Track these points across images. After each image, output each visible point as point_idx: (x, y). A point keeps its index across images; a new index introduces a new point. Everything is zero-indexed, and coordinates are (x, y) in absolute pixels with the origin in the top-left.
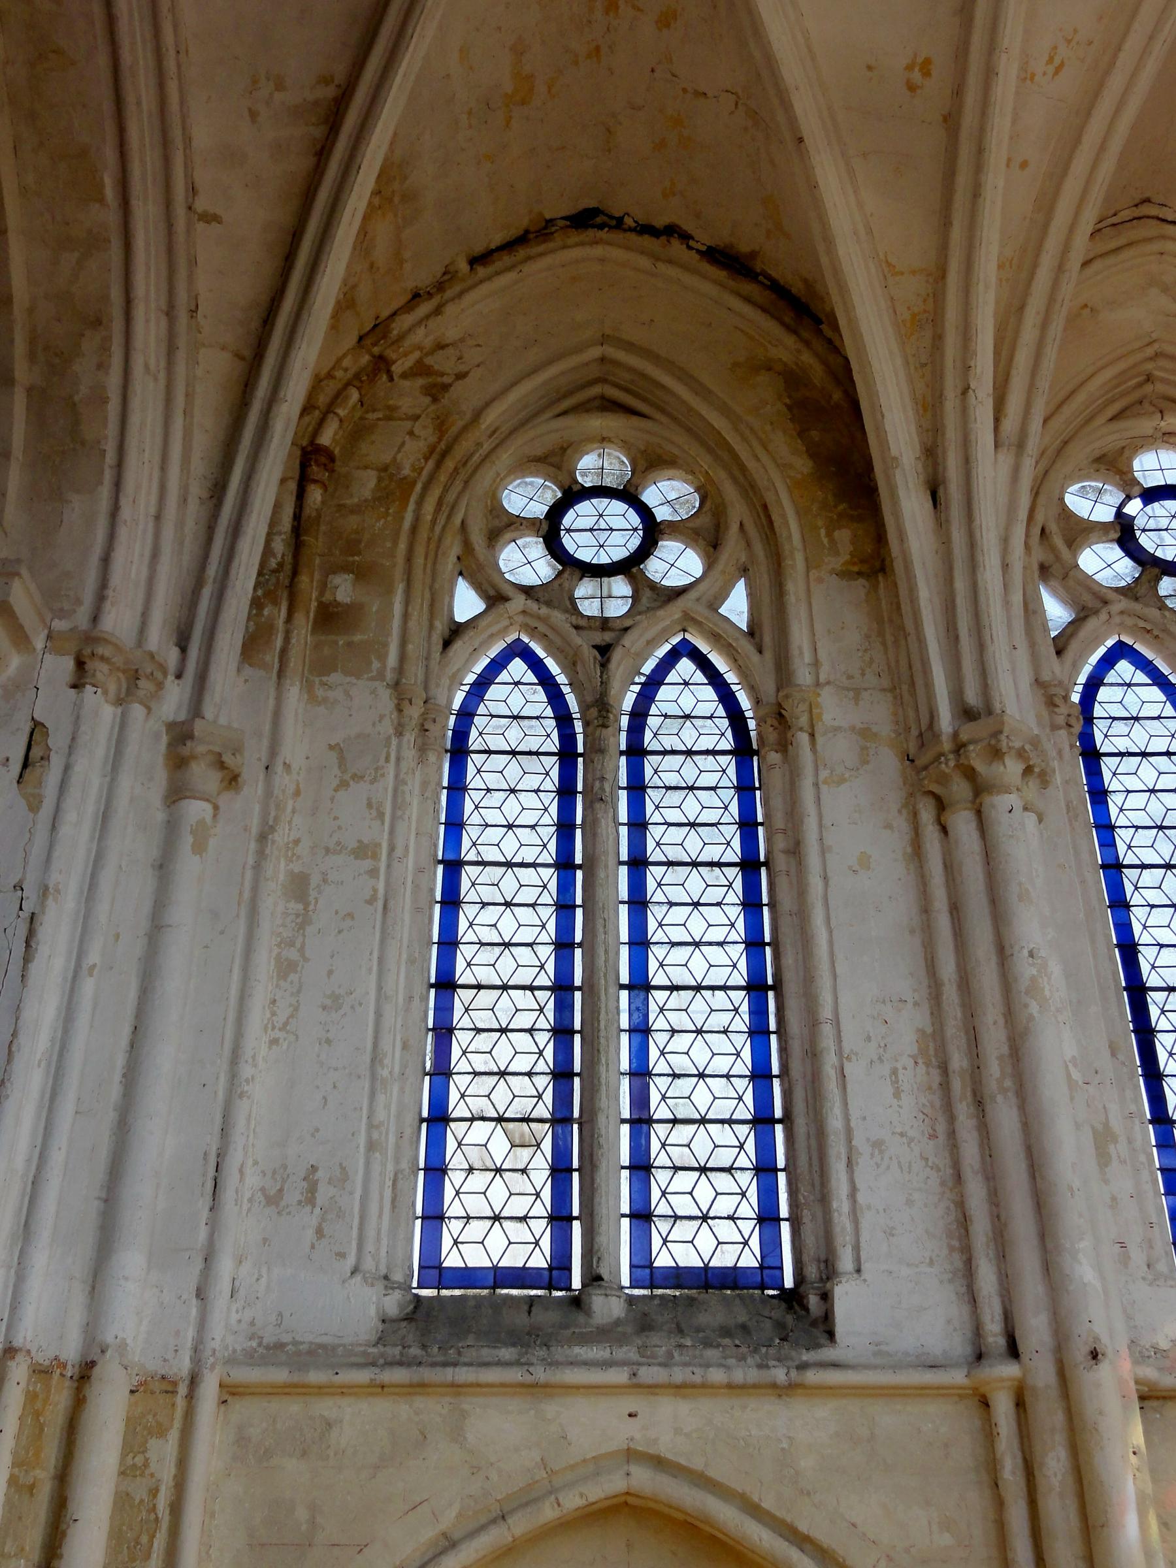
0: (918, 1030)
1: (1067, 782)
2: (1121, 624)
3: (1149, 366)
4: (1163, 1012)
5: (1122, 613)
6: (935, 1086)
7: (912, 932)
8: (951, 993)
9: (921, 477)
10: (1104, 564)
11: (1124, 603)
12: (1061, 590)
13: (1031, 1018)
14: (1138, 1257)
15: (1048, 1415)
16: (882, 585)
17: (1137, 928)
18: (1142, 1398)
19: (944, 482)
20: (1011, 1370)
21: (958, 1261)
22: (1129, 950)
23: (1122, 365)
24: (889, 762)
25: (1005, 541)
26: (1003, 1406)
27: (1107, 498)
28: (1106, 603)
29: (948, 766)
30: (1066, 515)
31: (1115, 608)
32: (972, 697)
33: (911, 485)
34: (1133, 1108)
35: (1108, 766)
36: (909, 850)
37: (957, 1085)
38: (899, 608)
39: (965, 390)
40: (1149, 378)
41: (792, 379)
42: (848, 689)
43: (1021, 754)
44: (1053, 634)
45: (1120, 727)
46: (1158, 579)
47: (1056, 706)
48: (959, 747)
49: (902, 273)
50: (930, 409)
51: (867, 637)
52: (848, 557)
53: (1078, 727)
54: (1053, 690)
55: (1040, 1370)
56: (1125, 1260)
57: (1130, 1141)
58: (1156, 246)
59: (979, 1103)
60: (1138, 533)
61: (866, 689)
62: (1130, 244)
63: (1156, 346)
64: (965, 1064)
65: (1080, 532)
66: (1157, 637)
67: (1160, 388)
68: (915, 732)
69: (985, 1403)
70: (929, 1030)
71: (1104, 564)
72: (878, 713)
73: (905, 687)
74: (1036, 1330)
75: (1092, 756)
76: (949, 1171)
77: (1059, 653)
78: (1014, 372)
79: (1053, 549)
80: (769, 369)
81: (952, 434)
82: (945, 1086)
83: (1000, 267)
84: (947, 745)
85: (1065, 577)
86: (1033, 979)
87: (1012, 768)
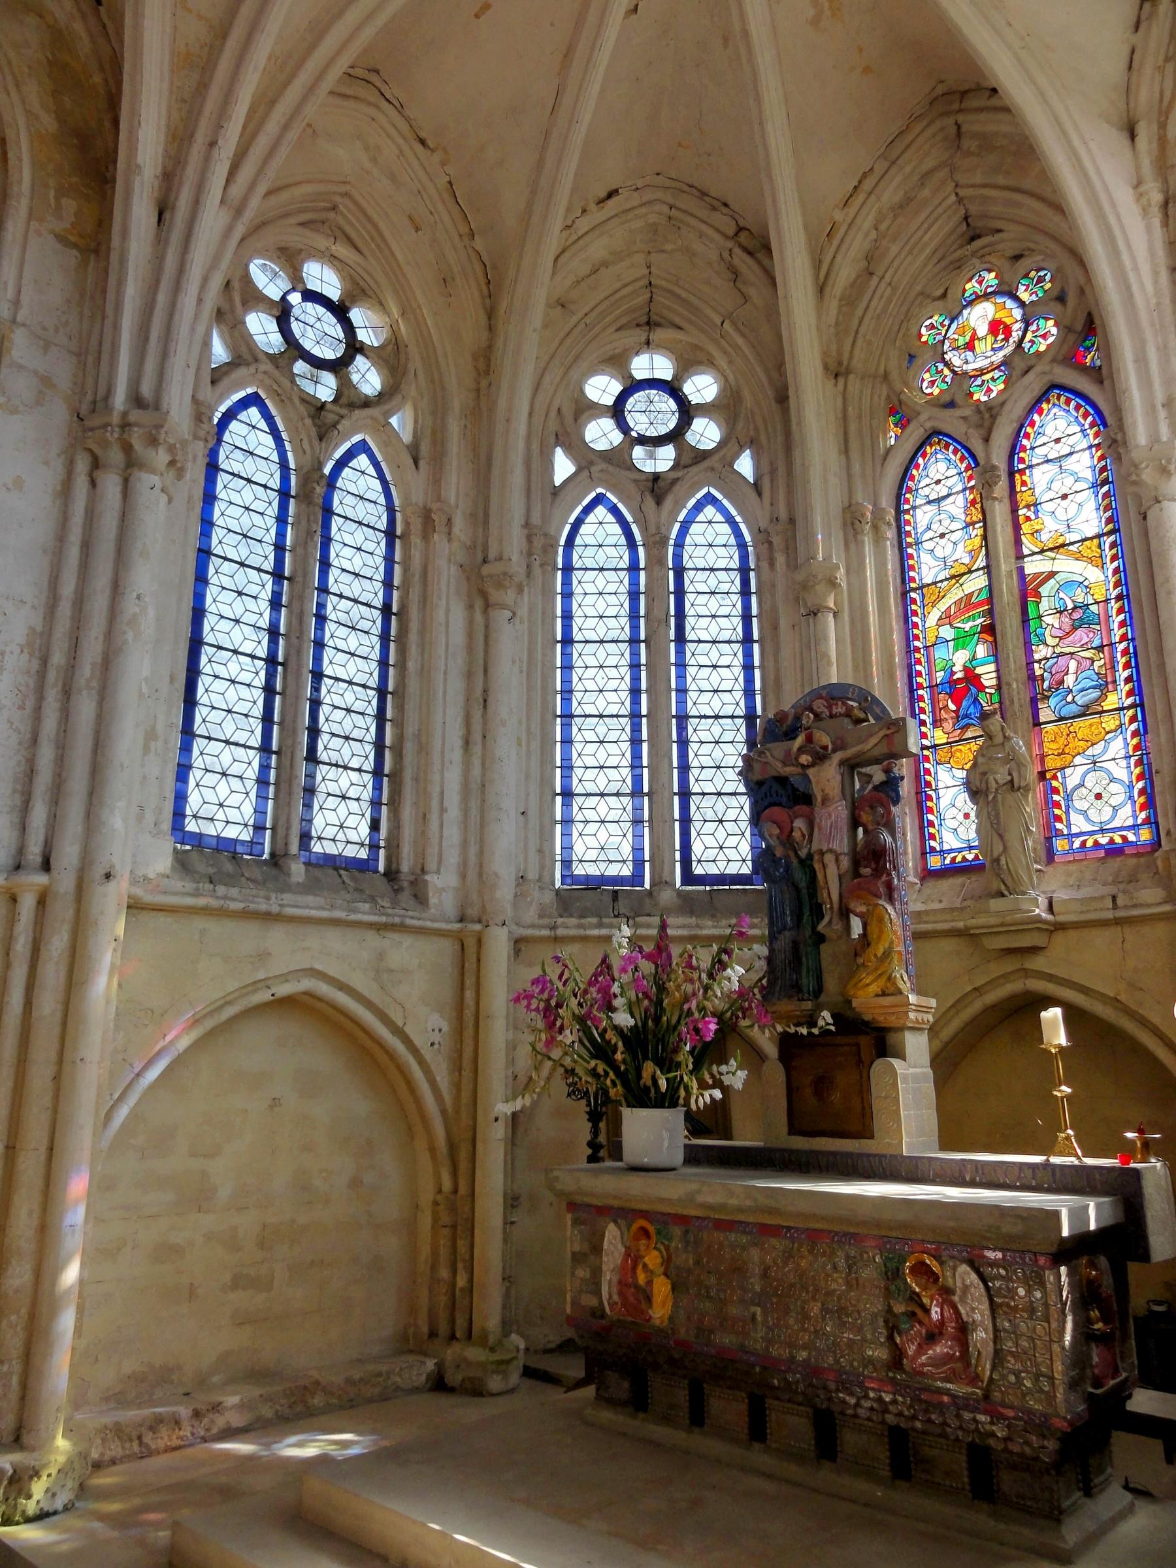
0: (30, 628)
1: (194, 481)
2: (262, 381)
3: (338, 199)
4: (210, 661)
5: (265, 373)
6: (33, 671)
7: (45, 551)
8: (65, 609)
9: (156, 194)
10: (262, 329)
11: (267, 366)
12: (227, 336)
13: (125, 642)
14: (150, 818)
15: (62, 911)
16: (92, 264)
17: (209, 600)
18: (128, 907)
19: (173, 208)
20: (42, 879)
21: (18, 800)
22: (198, 613)
23: (322, 188)
24: (59, 414)
25: (205, 280)
26: (28, 903)
27: (279, 281)
28: (256, 360)
29: (113, 435)
30: (247, 279)
31: (262, 367)
32: (146, 390)
33: (145, 194)
34: (174, 721)
35: (222, 479)
36: (59, 488)
37: (52, 675)
38: (104, 291)
39: (212, 144)
40: (334, 208)
41: (58, 38)
42: (40, 338)
43: (171, 449)
44: (213, 366)
45: (238, 454)
46: (295, 360)
47: (201, 422)
48: (125, 425)
49: (190, 11)
50: (179, 141)
51: (68, 301)
52: (68, 226)
53: (211, 445)
54: (203, 409)
55: (64, 879)
56: (140, 818)
57: (166, 742)
58: (372, 112)
59: (67, 693)
60: (292, 319)
61: (56, 345)
62: (356, 98)
63: (347, 188)
64: (63, 662)
65: (254, 298)
66: (283, 401)
67: (341, 222)
68: (89, 397)
69: (14, 899)
70: (39, 629)
71: (262, 329)
72: (63, 371)
73: (90, 359)
74: (68, 855)
75: (213, 469)
76: (28, 736)
77: (213, 382)
78: (252, 151)
79: (231, 300)
80: (41, 16)
81: (190, 173)
82: (42, 674)
83: (269, 59)
84: (116, 419)
85: (234, 327)
86: (135, 615)
87: (161, 457)
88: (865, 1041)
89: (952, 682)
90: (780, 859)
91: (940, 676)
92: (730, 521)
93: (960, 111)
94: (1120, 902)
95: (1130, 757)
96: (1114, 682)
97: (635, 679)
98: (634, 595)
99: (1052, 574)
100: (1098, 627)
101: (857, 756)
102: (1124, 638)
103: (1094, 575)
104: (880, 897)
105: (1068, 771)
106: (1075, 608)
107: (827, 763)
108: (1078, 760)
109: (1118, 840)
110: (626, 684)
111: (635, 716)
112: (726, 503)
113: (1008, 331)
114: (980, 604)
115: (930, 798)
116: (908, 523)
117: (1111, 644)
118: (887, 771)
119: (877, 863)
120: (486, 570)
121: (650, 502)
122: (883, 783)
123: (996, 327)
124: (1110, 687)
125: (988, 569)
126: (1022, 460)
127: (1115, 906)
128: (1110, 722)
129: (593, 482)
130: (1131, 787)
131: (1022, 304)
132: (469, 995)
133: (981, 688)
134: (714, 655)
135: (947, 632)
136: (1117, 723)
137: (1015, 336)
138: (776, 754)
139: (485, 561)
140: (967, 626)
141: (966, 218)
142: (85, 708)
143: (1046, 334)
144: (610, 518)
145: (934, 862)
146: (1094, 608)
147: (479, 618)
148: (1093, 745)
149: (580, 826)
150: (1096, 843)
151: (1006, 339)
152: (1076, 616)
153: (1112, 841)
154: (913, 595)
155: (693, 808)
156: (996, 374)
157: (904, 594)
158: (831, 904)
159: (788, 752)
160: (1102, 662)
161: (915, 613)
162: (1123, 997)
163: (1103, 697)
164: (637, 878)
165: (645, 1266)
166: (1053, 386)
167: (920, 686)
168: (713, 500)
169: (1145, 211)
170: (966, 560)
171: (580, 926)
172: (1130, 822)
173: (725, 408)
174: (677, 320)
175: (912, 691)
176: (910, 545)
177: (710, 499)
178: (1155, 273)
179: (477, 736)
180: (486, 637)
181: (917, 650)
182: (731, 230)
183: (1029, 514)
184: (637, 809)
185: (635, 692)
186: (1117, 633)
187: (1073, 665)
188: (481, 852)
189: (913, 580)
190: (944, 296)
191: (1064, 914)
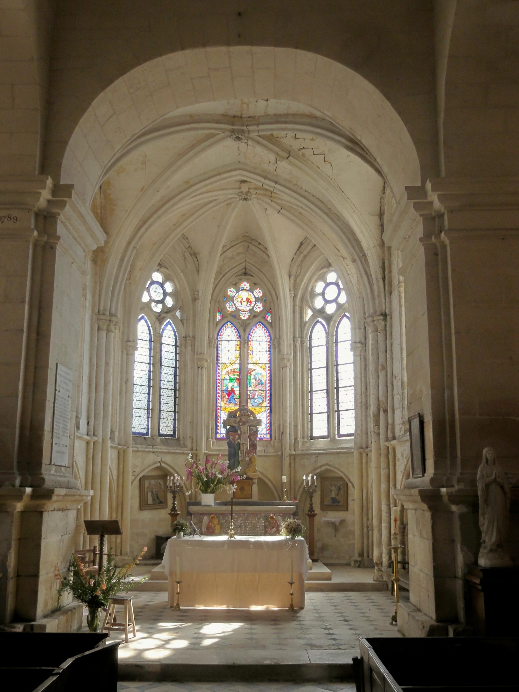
15: (99, 447)
88: (250, 481)
89: (227, 391)
91: (224, 388)
92: (174, 331)
93: (250, 243)
97: (150, 375)
98: (150, 349)
99: (254, 370)
103: (264, 373)
110: (147, 377)
111: (149, 386)
112: (173, 324)
113: (251, 303)
114: (237, 372)
115: (218, 419)
116: (220, 344)
120: (129, 344)
121: (157, 323)
123: (248, 300)
125: (241, 364)
126: (251, 338)
129: (143, 313)
130: (266, 425)
131: (255, 297)
132: (121, 466)
133: (235, 394)
134: (168, 371)
135: (227, 377)
137: (252, 305)
139: (128, 341)
140: (233, 377)
141: (245, 268)
142: (102, 395)
143: (259, 307)
144: (145, 324)
145: (218, 436)
147: (125, 356)
149: (134, 417)
151: (250, 304)
152: (259, 382)
154: (219, 364)
155: (161, 415)
156: (247, 313)
157: (217, 363)
161: (219, 369)
162: (264, 472)
164: (147, 434)
165: (214, 524)
166: (260, 322)
167: (219, 389)
168: (170, 324)
169: (290, 298)
170: (234, 359)
171: (142, 448)
173: (174, 295)
174: (168, 267)
175: (217, 390)
176: (219, 350)
177: (169, 323)
178: (291, 313)
179: (124, 393)
180: (127, 363)
181: (219, 380)
182: (187, 246)
183: (251, 353)
184: (148, 413)
185: (149, 379)
186: (268, 388)
187: (257, 393)
188: (125, 426)
189: (219, 360)
190: (236, 284)
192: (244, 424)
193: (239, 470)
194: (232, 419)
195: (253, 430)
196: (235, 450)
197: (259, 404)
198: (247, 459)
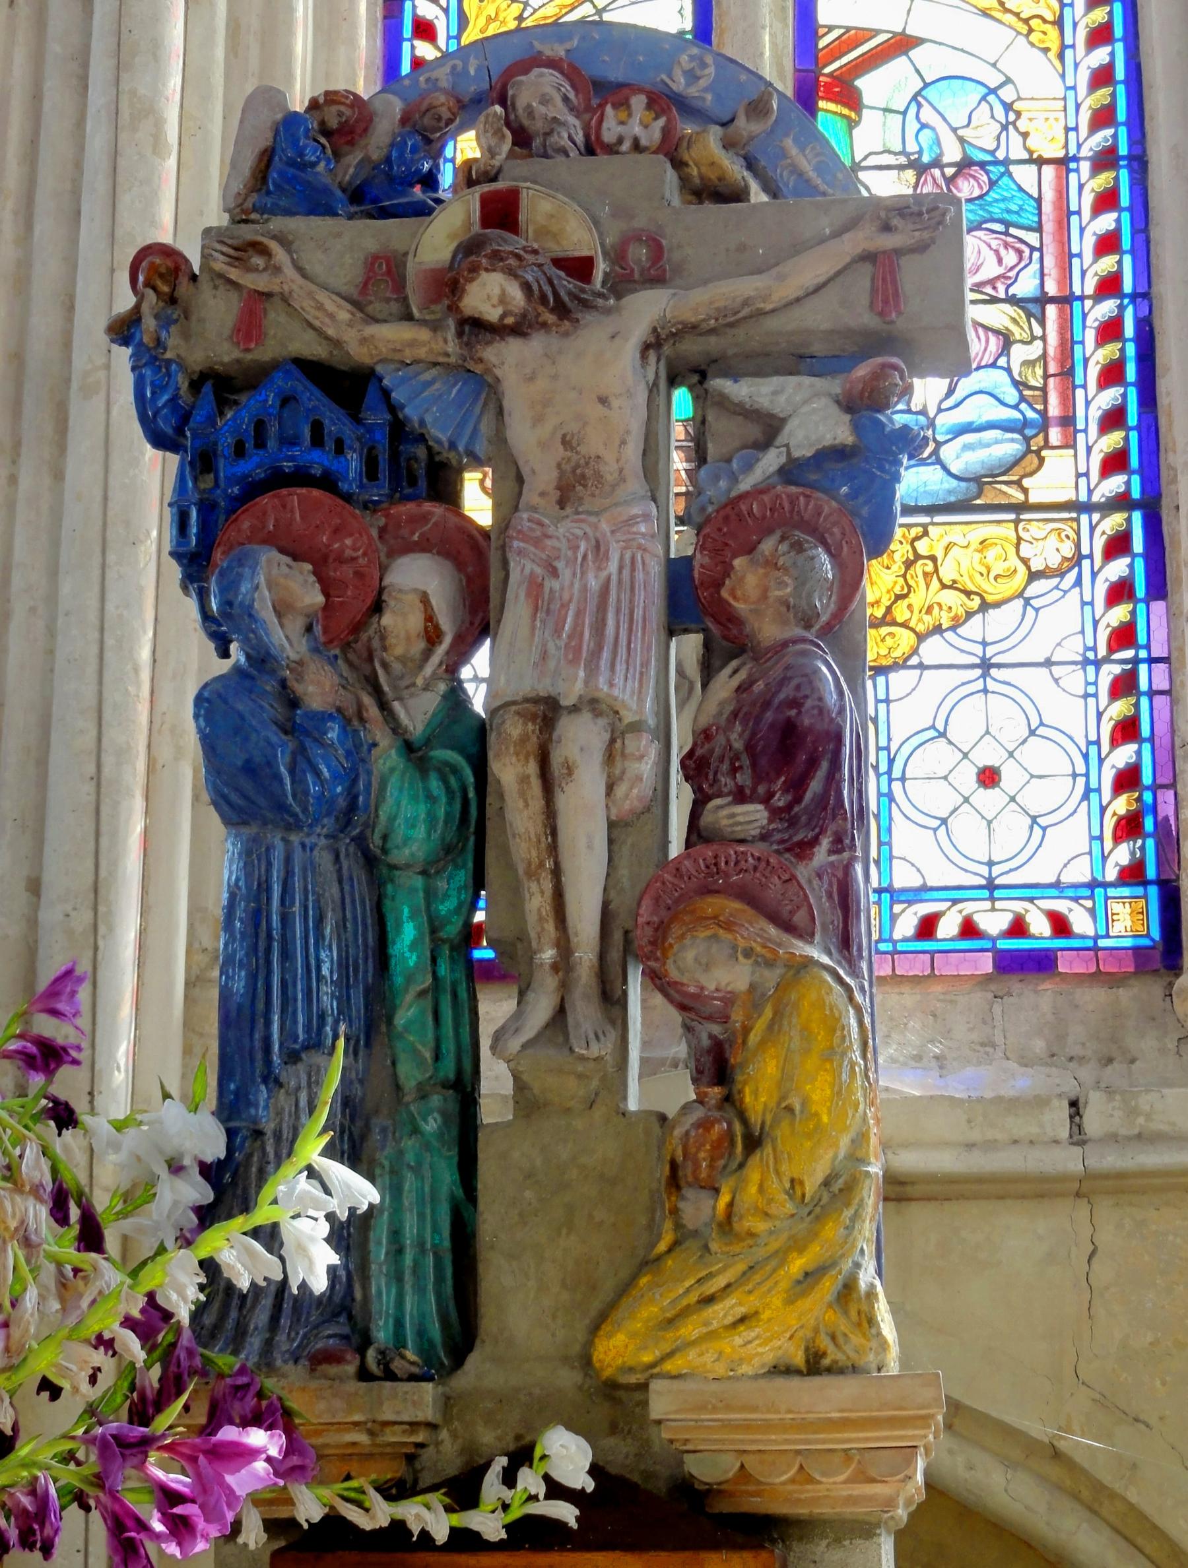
90: (322, 718)
94: (1093, 1122)
95: (1097, 664)
96: (1067, 421)
99: (902, 44)
100: (1032, 238)
101: (730, 320)
102: (1109, 286)
104: (807, 935)
105: (900, 681)
106: (965, 165)
107: (593, 333)
108: (933, 650)
109: (1039, 926)
117: (1065, 300)
118: (865, 403)
119: (797, 787)
122: (839, 453)
124: (1055, 435)
127: (1078, 1136)
128: (1047, 544)
136: (1068, 550)
138: (315, 261)
146: (1026, 175)
148: (985, 606)
150: (969, 929)
153: (1018, 928)
158: (565, 947)
159: (386, 271)
160: (1036, 349)
162: (1081, 1443)
163: (1031, 458)
172: (1080, 873)
191: (906, 1145)
192: (567, 293)
193: (315, 1264)
194: (328, 251)
195: (769, 428)
196: (374, 864)
197: (979, 481)
198: (653, 1074)
